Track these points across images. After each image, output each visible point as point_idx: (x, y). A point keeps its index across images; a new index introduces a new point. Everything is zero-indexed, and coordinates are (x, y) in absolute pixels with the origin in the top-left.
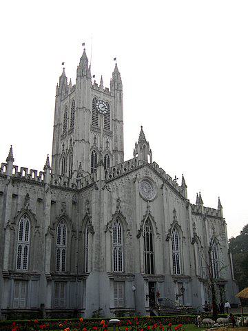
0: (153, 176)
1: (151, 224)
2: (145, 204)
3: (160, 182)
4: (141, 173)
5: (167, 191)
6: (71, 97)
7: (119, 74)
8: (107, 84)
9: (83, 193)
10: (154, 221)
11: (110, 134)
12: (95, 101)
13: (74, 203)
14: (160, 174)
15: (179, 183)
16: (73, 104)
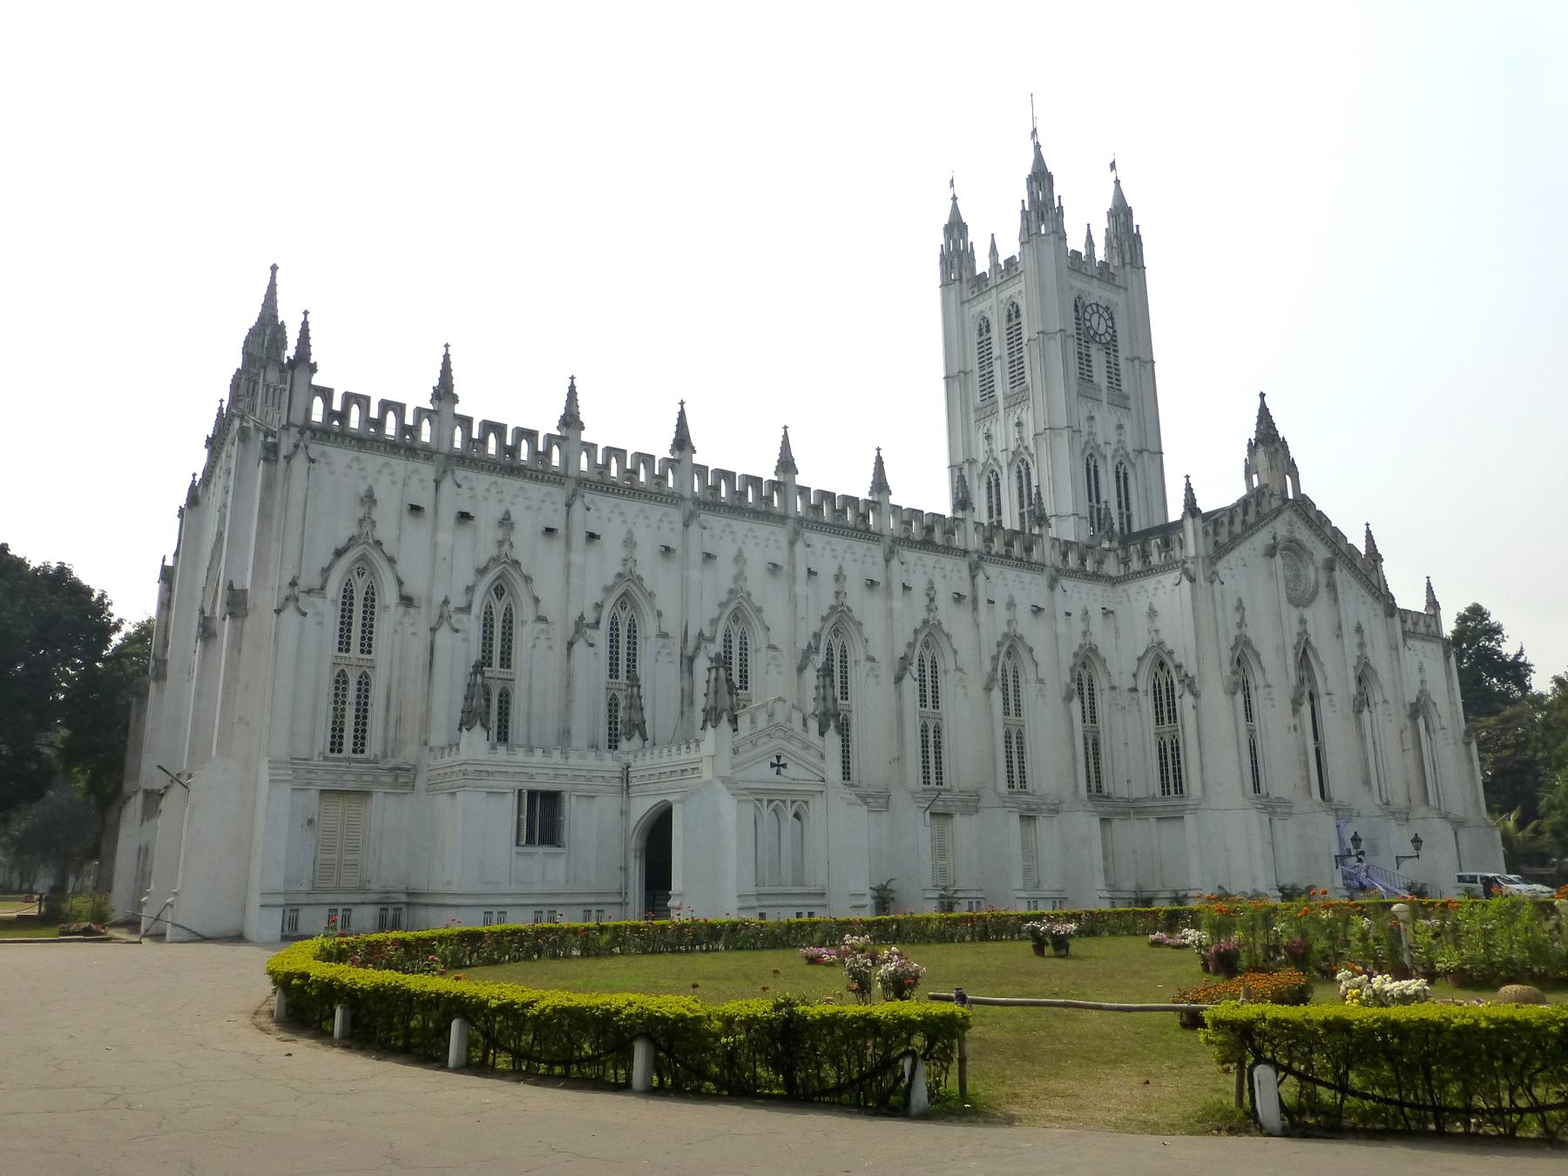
0: (1303, 534)
1: (1309, 667)
2: (1293, 614)
3: (1321, 553)
4: (1280, 527)
5: (1342, 576)
6: (1004, 295)
7: (1128, 212)
8: (1100, 254)
9: (1133, 587)
10: (1317, 657)
11: (1120, 401)
12: (1079, 307)
13: (1107, 613)
14: (1317, 522)
15: (1362, 550)
16: (1014, 313)
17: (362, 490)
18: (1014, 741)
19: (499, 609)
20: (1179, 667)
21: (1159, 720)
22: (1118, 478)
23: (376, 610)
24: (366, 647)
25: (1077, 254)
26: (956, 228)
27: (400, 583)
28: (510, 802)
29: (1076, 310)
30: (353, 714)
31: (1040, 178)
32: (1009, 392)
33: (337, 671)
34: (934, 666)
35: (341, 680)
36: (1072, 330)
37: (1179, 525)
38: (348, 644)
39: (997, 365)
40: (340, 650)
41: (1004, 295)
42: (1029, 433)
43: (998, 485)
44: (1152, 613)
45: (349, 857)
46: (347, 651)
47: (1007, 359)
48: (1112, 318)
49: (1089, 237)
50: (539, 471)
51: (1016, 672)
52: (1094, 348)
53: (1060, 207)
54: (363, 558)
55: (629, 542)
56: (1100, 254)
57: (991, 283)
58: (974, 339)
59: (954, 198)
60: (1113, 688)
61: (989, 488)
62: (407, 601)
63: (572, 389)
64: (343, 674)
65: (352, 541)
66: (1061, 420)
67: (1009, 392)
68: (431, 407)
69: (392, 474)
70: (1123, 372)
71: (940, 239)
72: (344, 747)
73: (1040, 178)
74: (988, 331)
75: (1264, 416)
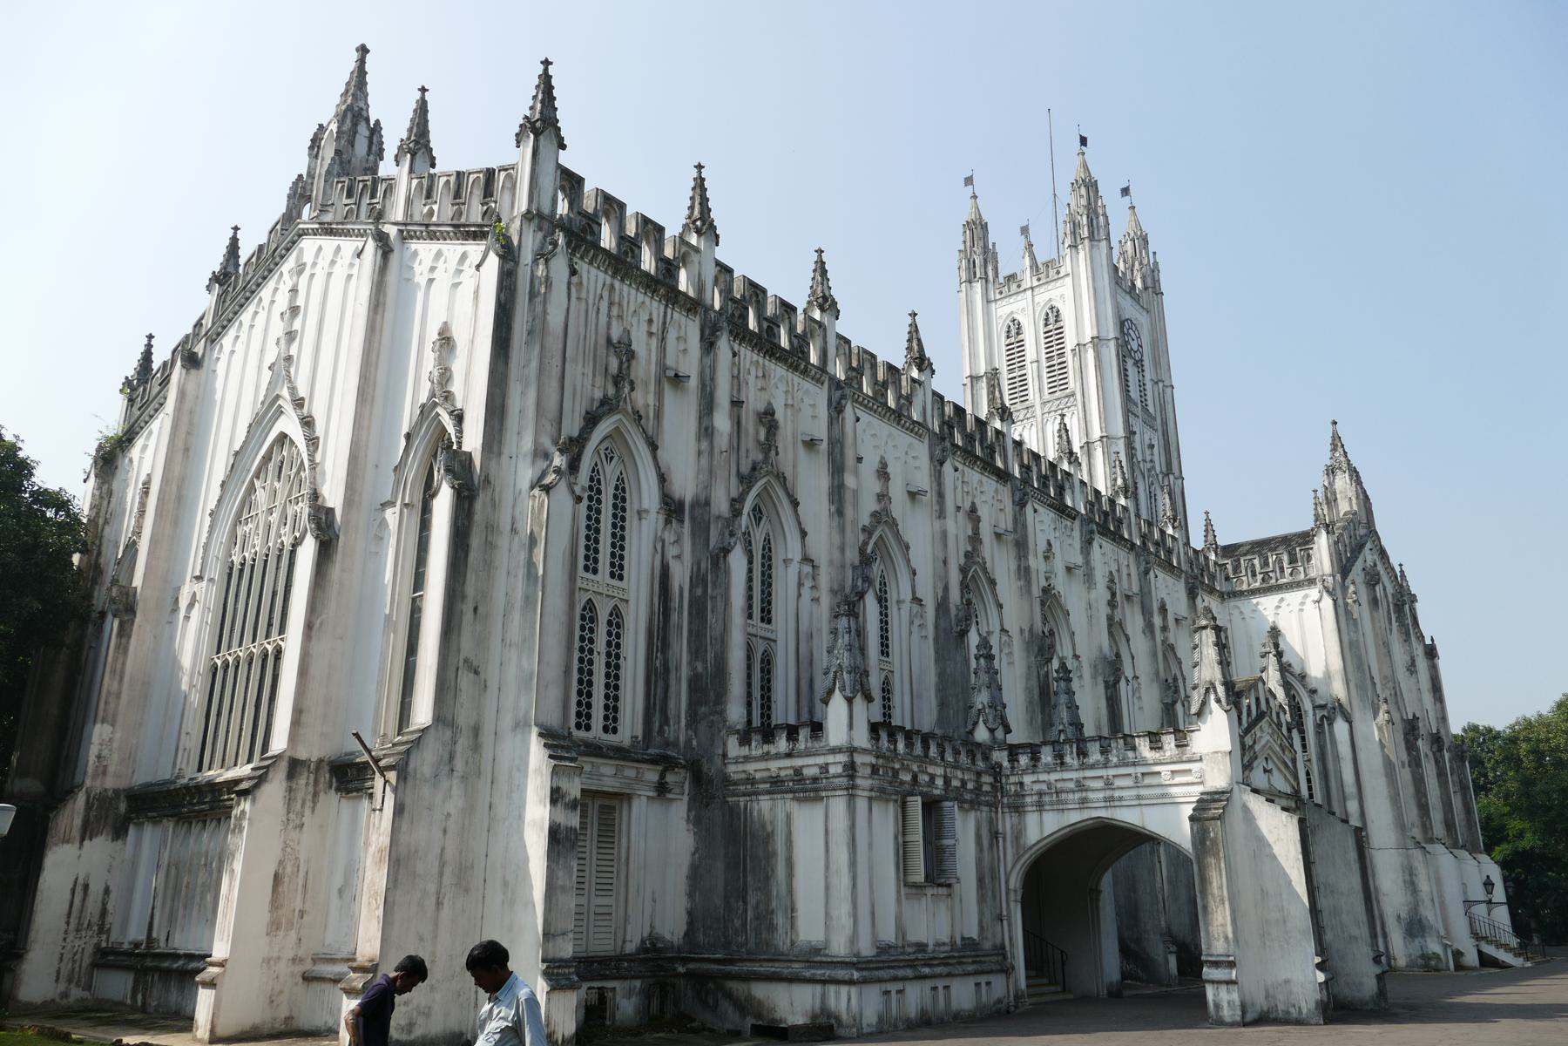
16: (1053, 317)
17: (616, 334)
20: (1313, 692)
23: (627, 515)
24: (617, 572)
26: (977, 229)
27: (662, 479)
30: (603, 670)
32: (1047, 396)
37: (1306, 538)
38: (596, 561)
39: (1030, 370)
44: (1275, 633)
45: (600, 901)
46: (595, 571)
47: (1044, 364)
50: (794, 359)
54: (616, 435)
55: (883, 474)
57: (1027, 283)
58: (1001, 342)
62: (672, 508)
64: (590, 606)
65: (607, 406)
67: (1047, 396)
69: (650, 321)
70: (1149, 393)
72: (593, 722)
75: (1336, 442)
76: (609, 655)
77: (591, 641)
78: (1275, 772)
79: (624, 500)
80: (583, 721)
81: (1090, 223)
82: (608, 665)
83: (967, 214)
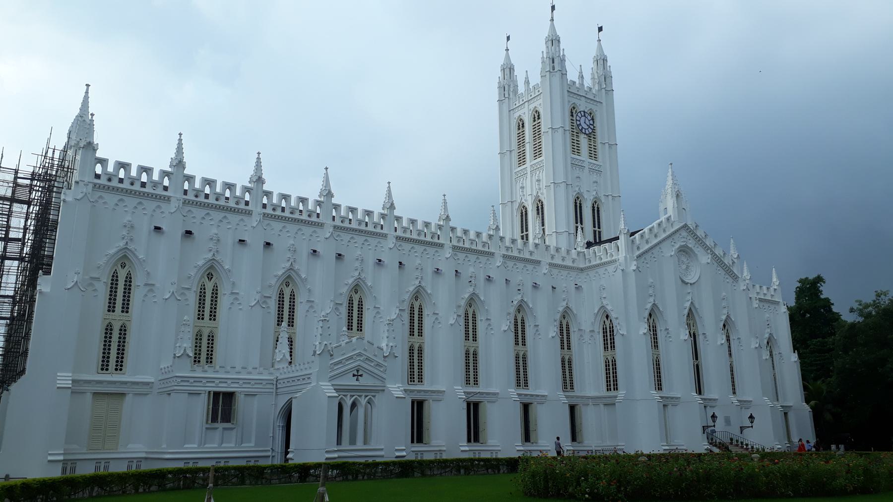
0: (691, 244)
7: (605, 60)
8: (588, 82)
13: (578, 288)
16: (537, 116)
18: (521, 359)
19: (209, 286)
21: (606, 348)
22: (593, 210)
23: (132, 288)
24: (126, 308)
25: (574, 83)
26: (508, 69)
28: (204, 398)
29: (572, 116)
31: (554, 40)
33: (107, 322)
34: (474, 316)
35: (109, 329)
36: (568, 127)
38: (114, 307)
40: (109, 311)
41: (532, 107)
42: (544, 183)
43: (526, 214)
46: (114, 311)
48: (593, 119)
49: (581, 72)
51: (523, 320)
52: (582, 136)
53: (564, 55)
56: (588, 82)
58: (515, 131)
59: (507, 50)
60: (580, 330)
61: (522, 216)
63: (259, 158)
66: (561, 179)
68: (170, 170)
71: (499, 74)
72: (110, 368)
73: (554, 40)
74: (523, 126)
76: (119, 342)
77: (110, 338)
78: (365, 375)
79: (130, 282)
80: (105, 367)
81: (555, 63)
82: (119, 346)
83: (502, 61)
